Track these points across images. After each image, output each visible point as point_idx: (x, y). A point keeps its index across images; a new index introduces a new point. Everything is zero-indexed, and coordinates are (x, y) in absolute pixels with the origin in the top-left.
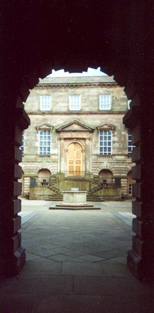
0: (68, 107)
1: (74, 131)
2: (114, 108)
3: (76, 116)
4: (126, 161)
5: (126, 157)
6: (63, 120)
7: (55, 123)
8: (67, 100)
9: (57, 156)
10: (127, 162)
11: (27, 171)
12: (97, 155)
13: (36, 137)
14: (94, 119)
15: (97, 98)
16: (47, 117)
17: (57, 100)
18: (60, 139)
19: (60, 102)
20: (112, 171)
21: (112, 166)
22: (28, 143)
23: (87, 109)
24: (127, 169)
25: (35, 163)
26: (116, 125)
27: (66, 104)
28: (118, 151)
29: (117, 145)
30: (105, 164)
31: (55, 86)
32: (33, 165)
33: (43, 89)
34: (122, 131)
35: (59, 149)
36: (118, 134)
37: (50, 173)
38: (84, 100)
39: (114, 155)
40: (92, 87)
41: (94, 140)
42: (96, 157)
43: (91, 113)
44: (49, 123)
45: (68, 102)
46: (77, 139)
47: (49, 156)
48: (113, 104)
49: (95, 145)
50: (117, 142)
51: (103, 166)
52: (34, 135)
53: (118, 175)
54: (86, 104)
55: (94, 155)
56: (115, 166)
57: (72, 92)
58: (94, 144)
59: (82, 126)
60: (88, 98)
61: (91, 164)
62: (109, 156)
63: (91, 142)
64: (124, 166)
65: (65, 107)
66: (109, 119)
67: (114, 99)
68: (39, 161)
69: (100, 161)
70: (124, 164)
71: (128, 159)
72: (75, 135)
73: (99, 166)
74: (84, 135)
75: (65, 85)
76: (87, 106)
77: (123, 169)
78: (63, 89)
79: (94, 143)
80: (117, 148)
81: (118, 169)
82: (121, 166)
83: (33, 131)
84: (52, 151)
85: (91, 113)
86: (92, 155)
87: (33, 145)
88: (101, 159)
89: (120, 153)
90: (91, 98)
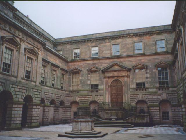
1: (115, 71)
2: (146, 51)
3: (117, 60)
4: (157, 92)
5: (157, 90)
6: (107, 63)
7: (102, 66)
8: (110, 49)
9: (103, 91)
10: (158, 93)
11: (82, 102)
13: (88, 77)
14: (131, 61)
15: (132, 45)
16: (95, 62)
17: (103, 49)
18: (105, 78)
19: (105, 50)
20: (146, 101)
21: (146, 97)
22: (83, 82)
23: (125, 54)
24: (158, 99)
25: (87, 97)
26: (148, 64)
27: (109, 52)
28: (151, 85)
29: (149, 80)
30: (141, 95)
31: (101, 39)
32: (85, 98)
33: (93, 42)
35: (104, 85)
37: (98, 103)
38: (122, 48)
39: (148, 88)
40: (128, 38)
41: (131, 77)
43: (128, 57)
44: (97, 66)
45: (111, 50)
46: (118, 77)
47: (97, 91)
48: (144, 48)
49: (132, 81)
50: (149, 78)
51: (139, 97)
52: (86, 75)
53: (152, 104)
54: (124, 50)
55: (132, 89)
56: (149, 97)
57: (113, 42)
58: (131, 80)
61: (129, 96)
62: (145, 89)
63: (128, 79)
64: (156, 97)
65: (109, 53)
66: (142, 60)
67: (145, 45)
68: (90, 95)
69: (137, 94)
70: (156, 95)
71: (159, 91)
72: (116, 74)
73: (136, 97)
74: (123, 74)
75: (108, 38)
76: (125, 52)
77: (155, 99)
78: (107, 41)
79: (131, 80)
80: (150, 83)
81: (152, 99)
82: (154, 97)
84: (99, 87)
85: (128, 57)
86: (130, 89)
88: (137, 92)
89: (152, 86)
90: (127, 45)
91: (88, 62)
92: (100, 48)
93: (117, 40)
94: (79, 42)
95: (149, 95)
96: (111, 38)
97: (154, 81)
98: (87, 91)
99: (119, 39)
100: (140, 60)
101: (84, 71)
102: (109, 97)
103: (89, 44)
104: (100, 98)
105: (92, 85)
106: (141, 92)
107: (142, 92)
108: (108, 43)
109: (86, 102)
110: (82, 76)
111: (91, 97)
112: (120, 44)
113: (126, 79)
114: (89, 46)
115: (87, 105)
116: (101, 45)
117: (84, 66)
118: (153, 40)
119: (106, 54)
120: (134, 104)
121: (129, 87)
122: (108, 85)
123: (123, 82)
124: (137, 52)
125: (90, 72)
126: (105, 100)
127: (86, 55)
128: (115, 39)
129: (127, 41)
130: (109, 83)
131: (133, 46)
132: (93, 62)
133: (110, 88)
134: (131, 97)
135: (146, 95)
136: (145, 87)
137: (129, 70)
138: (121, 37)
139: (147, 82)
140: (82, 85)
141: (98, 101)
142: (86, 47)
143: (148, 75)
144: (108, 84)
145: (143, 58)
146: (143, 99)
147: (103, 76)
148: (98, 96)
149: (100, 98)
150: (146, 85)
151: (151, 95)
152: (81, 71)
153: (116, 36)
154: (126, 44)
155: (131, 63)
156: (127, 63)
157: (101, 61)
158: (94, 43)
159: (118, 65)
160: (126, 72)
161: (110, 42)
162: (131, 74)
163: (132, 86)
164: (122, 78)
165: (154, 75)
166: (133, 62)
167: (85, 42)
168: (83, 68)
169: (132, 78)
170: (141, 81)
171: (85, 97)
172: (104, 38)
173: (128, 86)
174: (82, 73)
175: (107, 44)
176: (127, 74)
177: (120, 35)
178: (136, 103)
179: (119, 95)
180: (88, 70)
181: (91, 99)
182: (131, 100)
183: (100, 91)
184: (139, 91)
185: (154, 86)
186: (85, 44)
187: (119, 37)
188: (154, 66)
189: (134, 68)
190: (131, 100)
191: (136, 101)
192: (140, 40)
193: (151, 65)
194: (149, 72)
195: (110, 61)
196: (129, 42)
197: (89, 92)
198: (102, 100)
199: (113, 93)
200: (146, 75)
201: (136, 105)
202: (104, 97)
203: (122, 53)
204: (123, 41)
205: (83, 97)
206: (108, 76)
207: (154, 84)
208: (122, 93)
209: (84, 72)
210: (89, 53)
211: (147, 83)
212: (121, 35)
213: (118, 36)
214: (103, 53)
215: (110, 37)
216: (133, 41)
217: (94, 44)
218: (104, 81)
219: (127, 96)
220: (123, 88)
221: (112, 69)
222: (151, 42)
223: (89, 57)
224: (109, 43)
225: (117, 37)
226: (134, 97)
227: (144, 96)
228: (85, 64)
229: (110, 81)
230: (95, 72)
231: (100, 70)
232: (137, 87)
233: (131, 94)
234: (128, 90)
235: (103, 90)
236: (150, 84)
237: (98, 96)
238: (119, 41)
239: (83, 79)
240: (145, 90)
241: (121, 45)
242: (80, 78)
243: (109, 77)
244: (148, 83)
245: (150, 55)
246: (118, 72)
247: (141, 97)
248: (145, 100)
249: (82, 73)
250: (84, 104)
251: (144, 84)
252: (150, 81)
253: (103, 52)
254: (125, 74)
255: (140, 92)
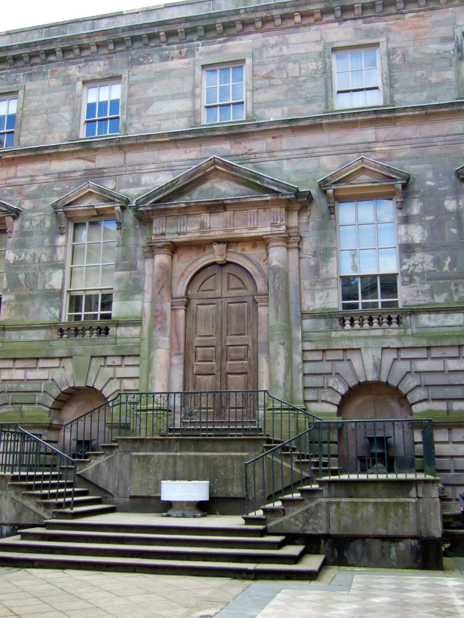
0: (195, 113)
1: (216, 207)
6: (170, 169)
7: (137, 184)
8: (187, 89)
9: (135, 331)
12: (326, 315)
13: (54, 247)
14: (310, 154)
15: (320, 65)
16: (102, 161)
17: (150, 93)
18: (151, 250)
20: (403, 389)
21: (404, 366)
22: (22, 277)
23: (274, 115)
25: (42, 363)
26: (411, 169)
28: (432, 292)
29: (423, 261)
30: (369, 356)
31: (139, 38)
32: (32, 375)
34: (444, 194)
35: (148, 296)
36: (425, 211)
39: (414, 312)
40: (297, 26)
41: (307, 246)
42: (322, 324)
43: (293, 126)
44: (109, 185)
45: (194, 96)
48: (391, 82)
49: (316, 270)
50: (424, 247)
51: (357, 364)
52: (47, 240)
53: (442, 406)
56: (421, 366)
57: (210, 53)
58: (312, 263)
59: (254, 183)
60: (279, 69)
61: (297, 359)
62: (395, 316)
65: (180, 114)
67: (397, 60)
68: (60, 353)
69: (346, 344)
72: (216, 225)
73: (341, 367)
75: (180, 28)
80: (427, 277)
83: (43, 222)
84: (117, 309)
86: (303, 315)
87: (40, 287)
89: (440, 300)
90: (290, 65)
91: (57, 166)
92: (130, 85)
93: (230, 44)
94: (16, 59)
95: (423, 354)
96: (194, 30)
97: (451, 266)
98: (43, 332)
99: (241, 33)
100: (368, 148)
101: (37, 216)
102: (171, 364)
103: (73, 70)
104: (121, 372)
105: (75, 302)
106: (373, 333)
107: (379, 332)
108: (179, 58)
109: (38, 398)
110: (21, 246)
111: (68, 363)
112: (249, 61)
113: (277, 254)
114: (68, 81)
115: (40, 412)
116: (141, 68)
117: (34, 188)
118: (444, 31)
119: (168, 116)
120: (325, 409)
121: (300, 302)
122: (167, 298)
123: (264, 276)
124: (344, 103)
125: (69, 218)
126: (149, 380)
127: (50, 125)
128: (220, 35)
129: (288, 45)
130: (175, 282)
131: (326, 73)
132: (91, 165)
133: (181, 313)
134: (309, 368)
135: (403, 355)
136: (395, 304)
137: (299, 201)
138: (252, 23)
139: (410, 277)
140: (19, 298)
141: (107, 392)
142: (54, 82)
143: (417, 234)
144: (171, 288)
145: (384, 132)
146: (384, 379)
147: (142, 242)
148: (109, 361)
149: (121, 372)
150: (404, 296)
151: (435, 353)
152: (16, 214)
153: (225, 20)
154: (287, 59)
155: (310, 164)
156: (286, 166)
157: (133, 157)
158: (102, 63)
159: (232, 173)
160: (280, 211)
161: (191, 53)
162: (307, 224)
163: (313, 299)
164: (257, 253)
165: (454, 231)
166: (325, 160)
167: (52, 58)
168: (28, 197)
169: (315, 254)
170: (368, 268)
171: (32, 364)
172: (155, 30)
173: (293, 298)
174: (22, 227)
175: (171, 64)
176: (288, 228)
177: (246, 11)
178: (337, 400)
179: (233, 355)
180: (55, 206)
181: (65, 376)
182: (311, 381)
183: (121, 331)
184: (357, 326)
185: (456, 298)
186: (49, 69)
187: (245, 24)
188: (454, 178)
189: (330, 191)
190: (311, 381)
191: (342, 390)
192: (367, 36)
193: (430, 175)
194: (420, 216)
195: (185, 157)
196: (302, 50)
197: (56, 336)
198: (129, 385)
199: (197, 340)
200: (402, 229)
201: (339, 413)
202: (145, 362)
203: (258, 112)
204: (265, 46)
205: (19, 364)
206: (168, 237)
207: (453, 288)
208: (255, 341)
209: (35, 223)
210: (68, 116)
211: (411, 281)
212: (255, 10)
213: (233, 19)
214: (152, 111)
215: (188, 25)
216: (325, 45)
217: (99, 69)
218: (148, 271)
219: (281, 360)
220: (262, 311)
221: (196, 196)
222: (433, 47)
223: (65, 136)
224: (186, 61)
225: (232, 25)
226: (326, 367)
227: (389, 357)
228: (42, 178)
229: (187, 264)
230: (96, 218)
231: (123, 208)
232: (345, 307)
233: (308, 346)
234: (288, 321)
235: (137, 323)
236: (427, 287)
237: (105, 357)
238: (240, 46)
239: (24, 262)
240: (398, 322)
241: (253, 65)
242: (10, 256)
243: (174, 248)
244: (417, 278)
245: (428, 113)
246: (228, 214)
247: (369, 366)
248: (393, 382)
249: (22, 227)
250: (25, 407)
251: (389, 284)
252: (429, 266)
253: (148, 104)
254: (273, 225)
255: (363, 333)
